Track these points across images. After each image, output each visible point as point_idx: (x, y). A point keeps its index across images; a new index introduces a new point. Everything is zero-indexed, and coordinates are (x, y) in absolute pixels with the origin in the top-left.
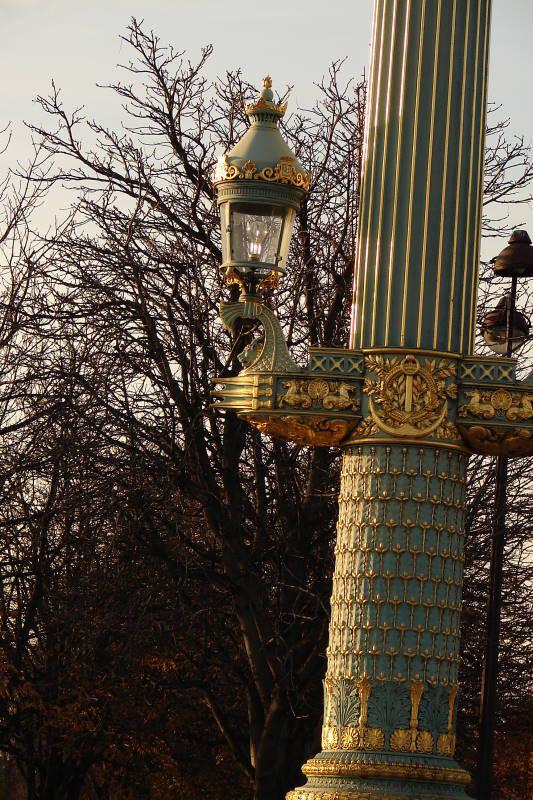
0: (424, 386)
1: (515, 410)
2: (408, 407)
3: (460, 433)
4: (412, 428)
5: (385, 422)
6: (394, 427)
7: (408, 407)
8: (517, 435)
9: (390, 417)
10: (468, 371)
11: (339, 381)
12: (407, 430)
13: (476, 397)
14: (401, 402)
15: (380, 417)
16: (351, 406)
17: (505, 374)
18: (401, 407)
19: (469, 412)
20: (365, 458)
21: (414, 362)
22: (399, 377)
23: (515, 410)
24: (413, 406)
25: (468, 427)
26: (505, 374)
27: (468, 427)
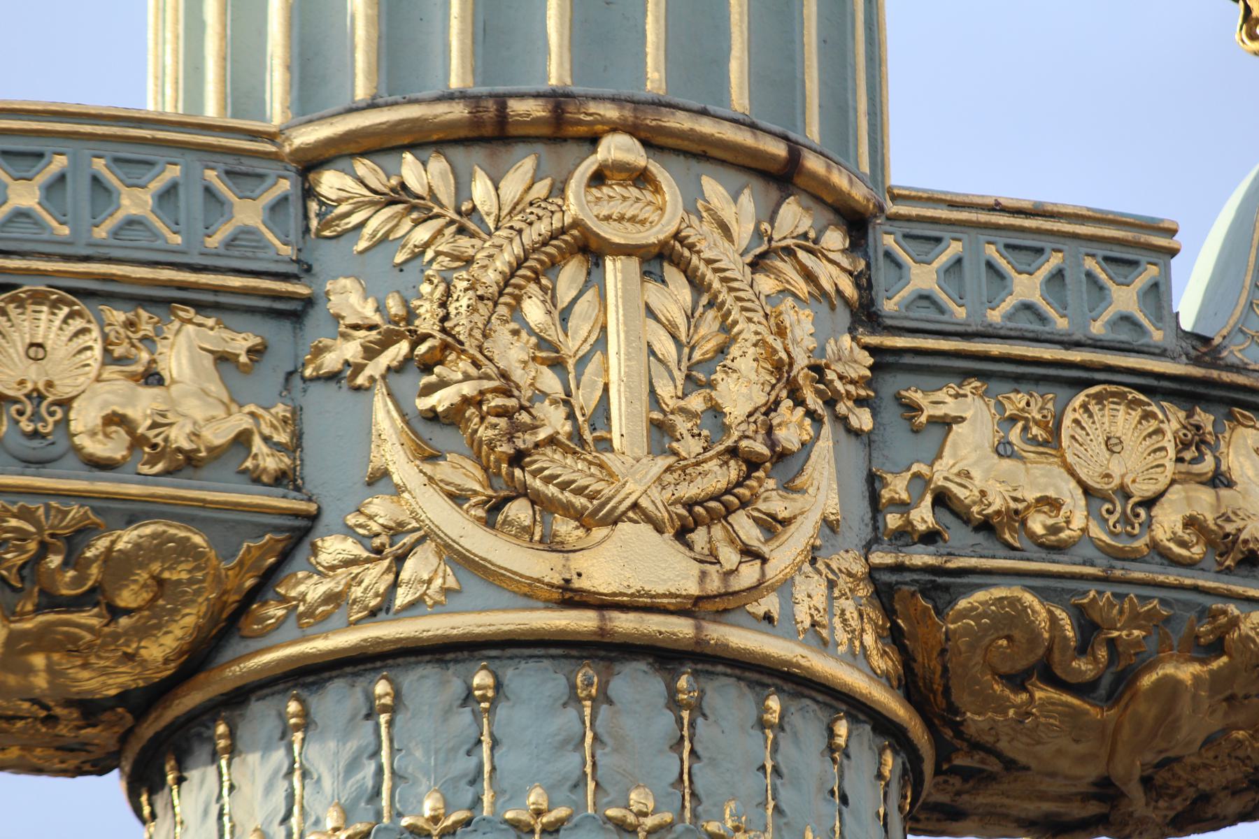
0: (710, 323)
1: (1204, 502)
2: (625, 424)
3: (894, 637)
4: (665, 545)
5: (492, 513)
6: (551, 544)
7: (625, 424)
8: (1217, 647)
9: (523, 492)
10: (923, 277)
11: (162, 301)
12: (630, 562)
13: (973, 416)
14: (586, 399)
15: (458, 498)
16: (242, 440)
17: (1125, 298)
18: (590, 434)
19: (942, 500)
20: (323, 756)
21: (642, 178)
22: (553, 265)
23: (1204, 502)
24: (661, 430)
25: (941, 586)
26: (1125, 298)
27: (941, 586)
